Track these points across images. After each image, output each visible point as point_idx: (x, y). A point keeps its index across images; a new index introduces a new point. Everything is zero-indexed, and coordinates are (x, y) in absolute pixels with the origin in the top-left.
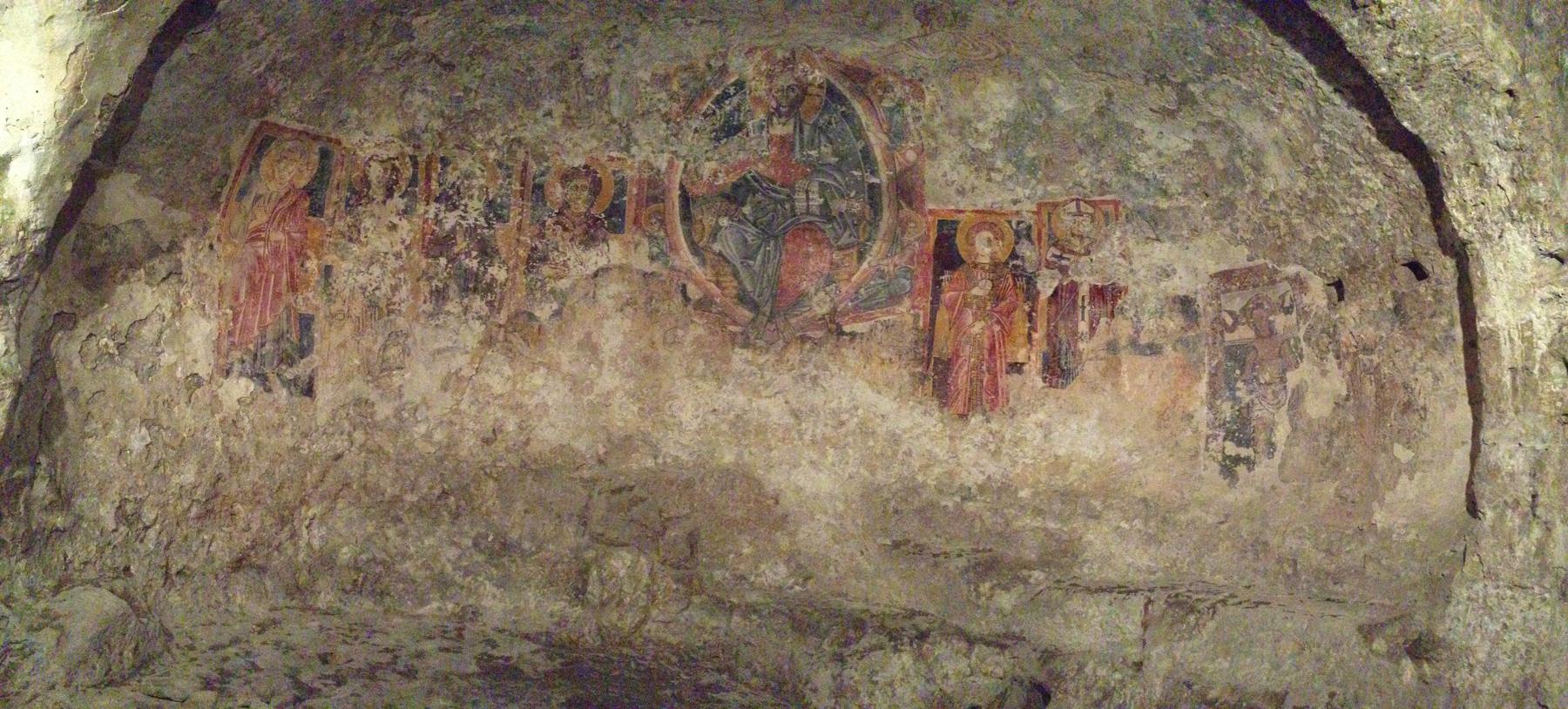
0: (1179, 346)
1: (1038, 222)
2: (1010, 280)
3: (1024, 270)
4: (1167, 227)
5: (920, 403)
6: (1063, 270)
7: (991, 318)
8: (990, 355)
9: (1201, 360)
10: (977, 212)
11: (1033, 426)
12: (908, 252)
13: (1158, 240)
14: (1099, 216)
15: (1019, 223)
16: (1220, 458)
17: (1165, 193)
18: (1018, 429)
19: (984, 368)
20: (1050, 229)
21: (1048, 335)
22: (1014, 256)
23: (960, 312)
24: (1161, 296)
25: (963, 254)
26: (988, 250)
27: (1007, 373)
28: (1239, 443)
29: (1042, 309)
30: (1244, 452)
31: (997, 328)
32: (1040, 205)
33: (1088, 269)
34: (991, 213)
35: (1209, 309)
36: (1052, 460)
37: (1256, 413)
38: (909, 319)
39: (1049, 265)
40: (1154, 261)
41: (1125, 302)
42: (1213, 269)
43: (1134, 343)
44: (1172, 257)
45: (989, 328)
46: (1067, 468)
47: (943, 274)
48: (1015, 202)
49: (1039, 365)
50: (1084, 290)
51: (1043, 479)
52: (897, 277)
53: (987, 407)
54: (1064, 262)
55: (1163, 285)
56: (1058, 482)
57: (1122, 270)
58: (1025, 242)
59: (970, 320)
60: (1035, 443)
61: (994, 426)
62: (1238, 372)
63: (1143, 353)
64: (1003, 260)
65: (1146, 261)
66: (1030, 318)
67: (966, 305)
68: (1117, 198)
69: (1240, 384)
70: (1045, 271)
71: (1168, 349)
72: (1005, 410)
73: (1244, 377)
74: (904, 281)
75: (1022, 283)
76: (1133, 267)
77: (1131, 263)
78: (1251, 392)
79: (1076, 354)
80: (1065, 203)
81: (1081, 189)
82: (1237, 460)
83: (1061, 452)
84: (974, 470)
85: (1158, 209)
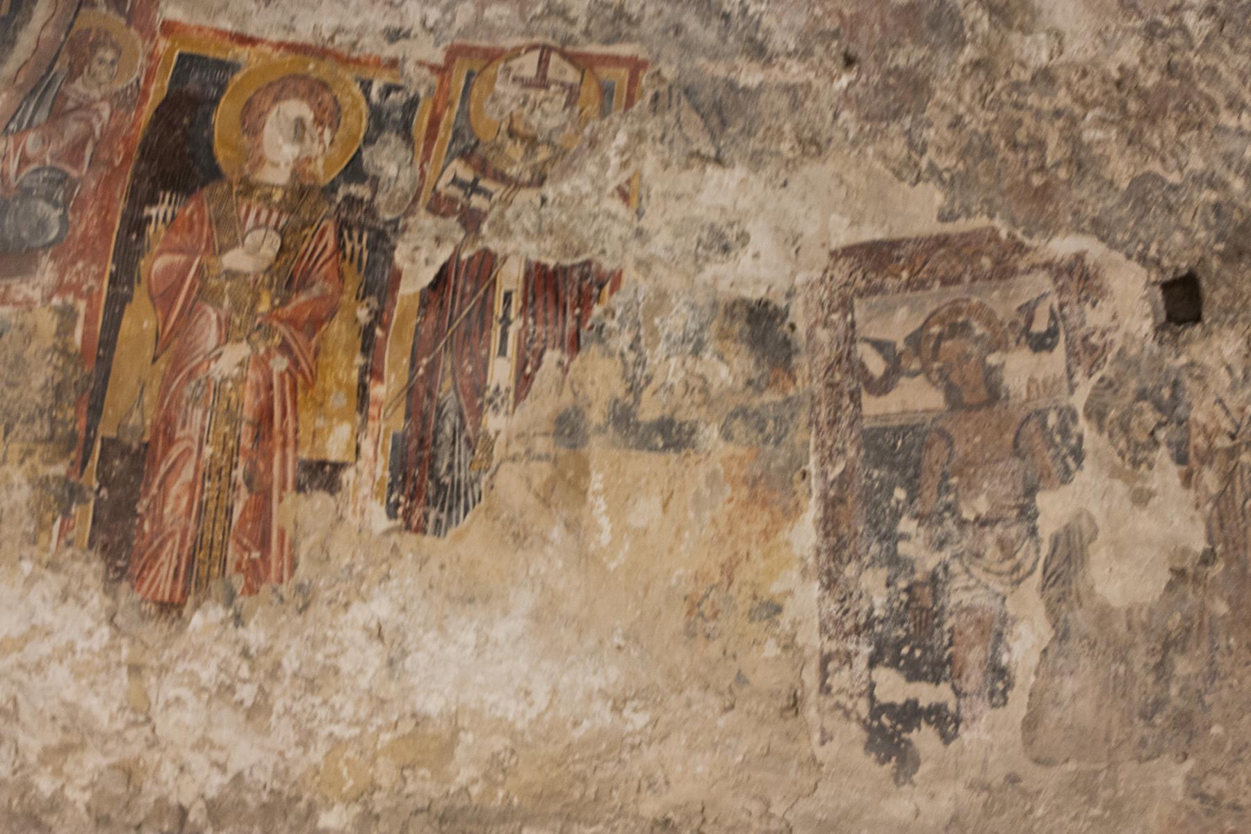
0: (738, 427)
1: (441, 98)
2: (330, 237)
3: (371, 211)
4: (748, 132)
5: (53, 566)
6: (471, 221)
7: (269, 333)
8: (257, 438)
9: (796, 465)
10: (293, 48)
11: (361, 638)
12: (73, 128)
13: (719, 161)
14: (590, 91)
15: (388, 90)
16: (863, 707)
17: (758, 51)
18: (314, 644)
19: (239, 473)
20: (464, 113)
21: (411, 391)
22: (354, 170)
23: (189, 313)
24: (701, 298)
25: (222, 155)
26: (289, 151)
27: (299, 488)
28: (913, 673)
29: (403, 319)
30: (927, 694)
31: (280, 364)
32: (454, 53)
33: (529, 221)
34: (321, 53)
35: (823, 335)
36: (407, 727)
37: (957, 595)
38: (47, 322)
39: (438, 206)
40: (697, 212)
41: (610, 312)
42: (843, 236)
43: (622, 418)
44: (743, 203)
45: (262, 362)
46: (447, 748)
47: (153, 201)
48: (394, 35)
49: (382, 470)
50: (511, 277)
51: (385, 782)
52: (26, 193)
53: (238, 582)
54: (477, 201)
55: (710, 271)
56: (423, 786)
57: (617, 230)
58: (393, 139)
59: (211, 336)
60: (364, 683)
61: (255, 635)
62: (900, 494)
63: (644, 444)
64: (324, 181)
65: (677, 211)
66: (368, 342)
67: (204, 293)
68: (643, 55)
69: (906, 525)
70: (424, 220)
71: (710, 434)
72: (284, 589)
73: (918, 506)
74: (42, 207)
75: (357, 244)
76: (644, 223)
77: (639, 214)
78: (941, 545)
79: (479, 443)
80: (516, 52)
81: (559, 24)
82: (910, 714)
83: (433, 705)
84: (198, 761)
85: (731, 85)
